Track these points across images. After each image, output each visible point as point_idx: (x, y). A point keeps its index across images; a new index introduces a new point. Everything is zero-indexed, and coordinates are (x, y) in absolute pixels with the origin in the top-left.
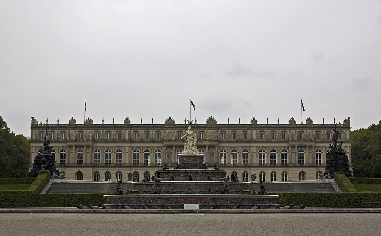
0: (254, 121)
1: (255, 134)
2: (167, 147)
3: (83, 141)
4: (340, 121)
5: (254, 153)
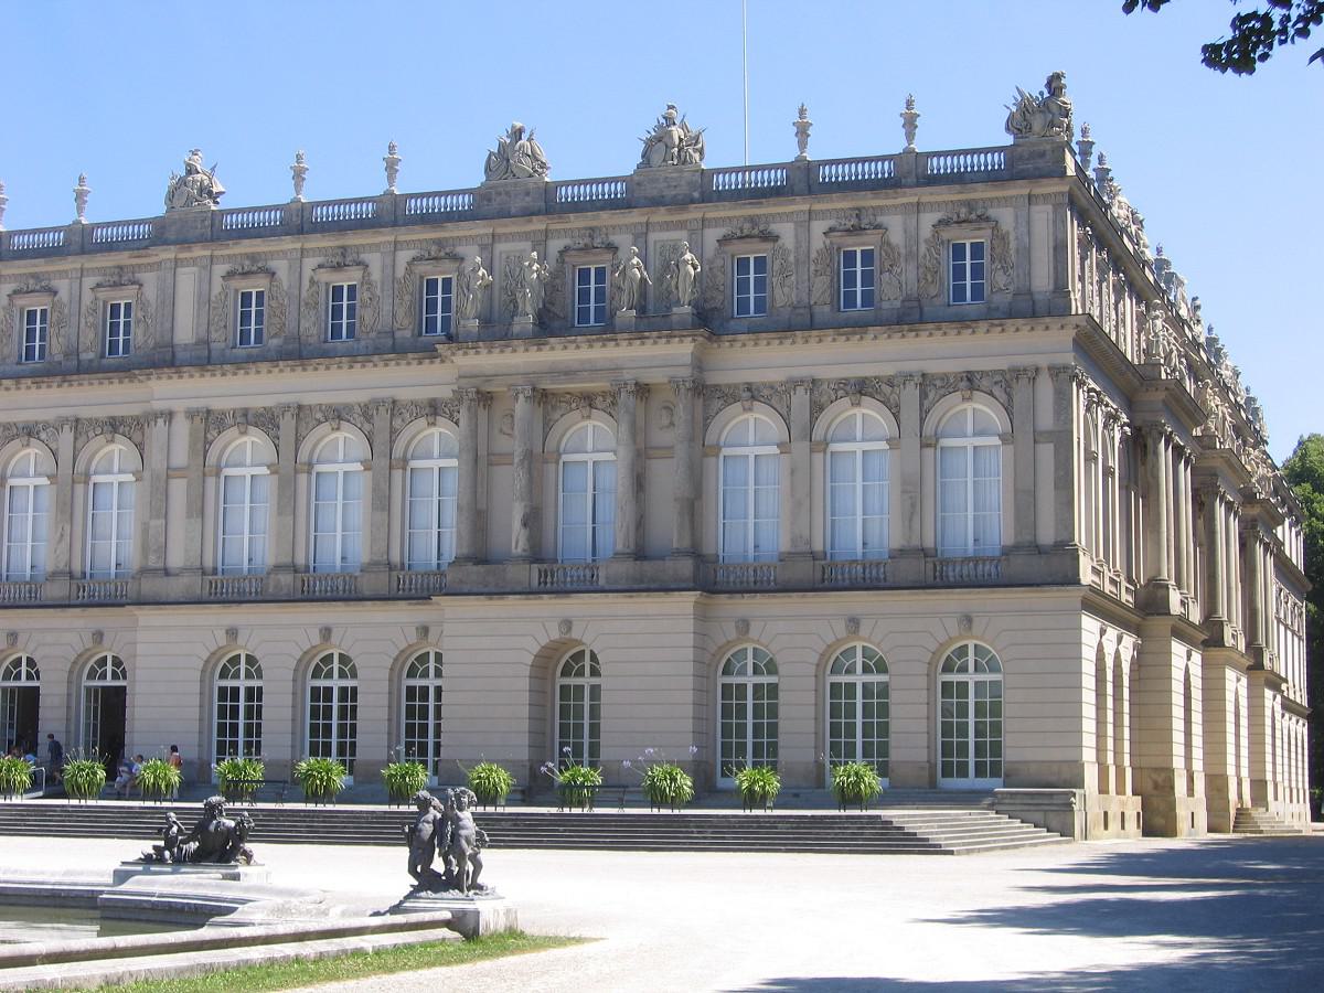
4: (971, 124)
5: (171, 472)
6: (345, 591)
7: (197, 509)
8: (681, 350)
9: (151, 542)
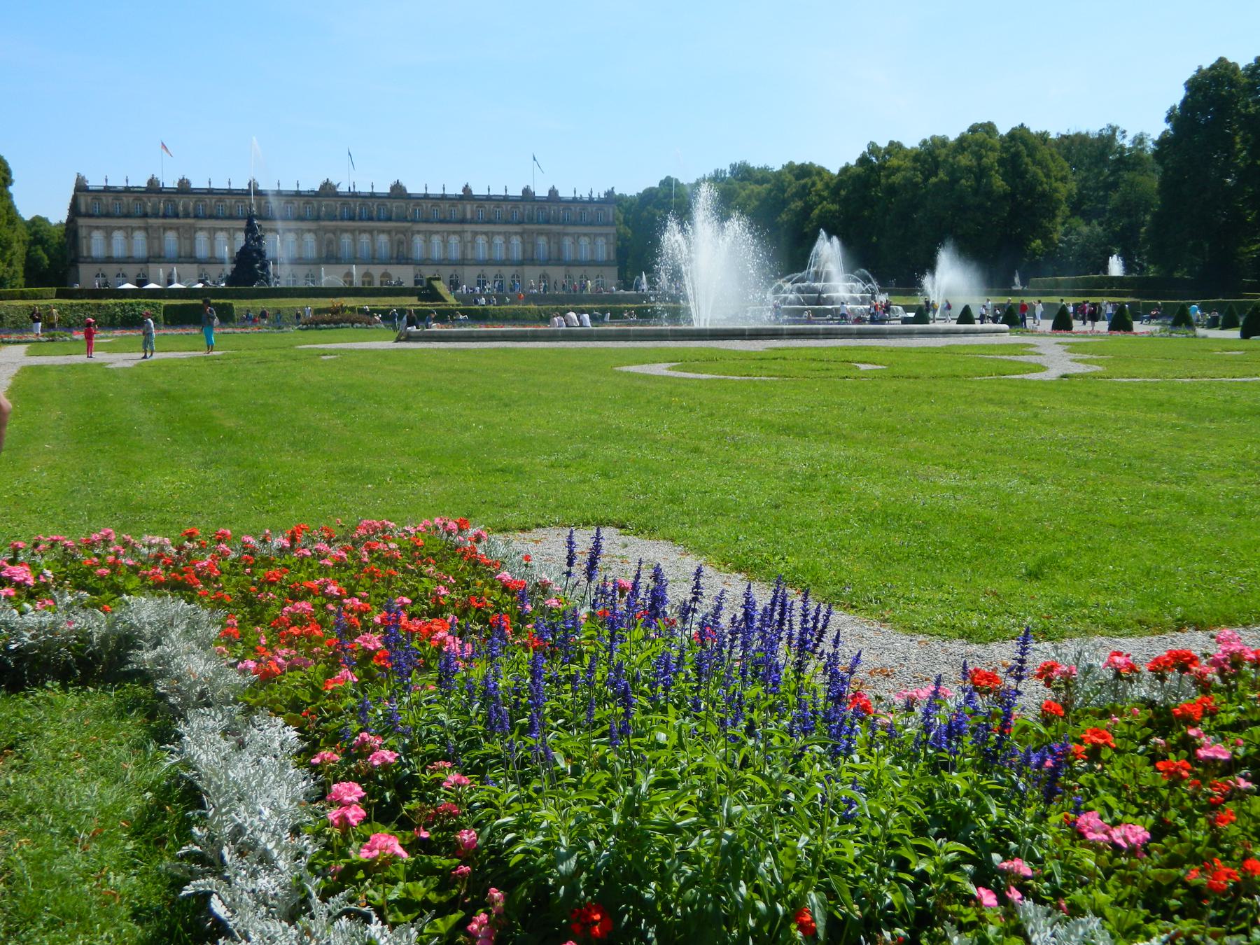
0: (466, 189)
1: (469, 209)
2: (326, 231)
3: (177, 216)
6: (503, 263)
7: (473, 248)
8: (561, 227)
9: (463, 253)
